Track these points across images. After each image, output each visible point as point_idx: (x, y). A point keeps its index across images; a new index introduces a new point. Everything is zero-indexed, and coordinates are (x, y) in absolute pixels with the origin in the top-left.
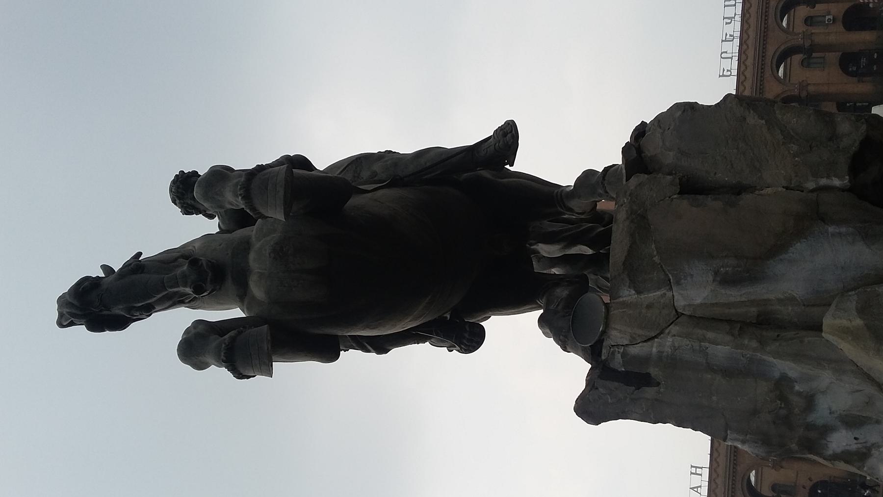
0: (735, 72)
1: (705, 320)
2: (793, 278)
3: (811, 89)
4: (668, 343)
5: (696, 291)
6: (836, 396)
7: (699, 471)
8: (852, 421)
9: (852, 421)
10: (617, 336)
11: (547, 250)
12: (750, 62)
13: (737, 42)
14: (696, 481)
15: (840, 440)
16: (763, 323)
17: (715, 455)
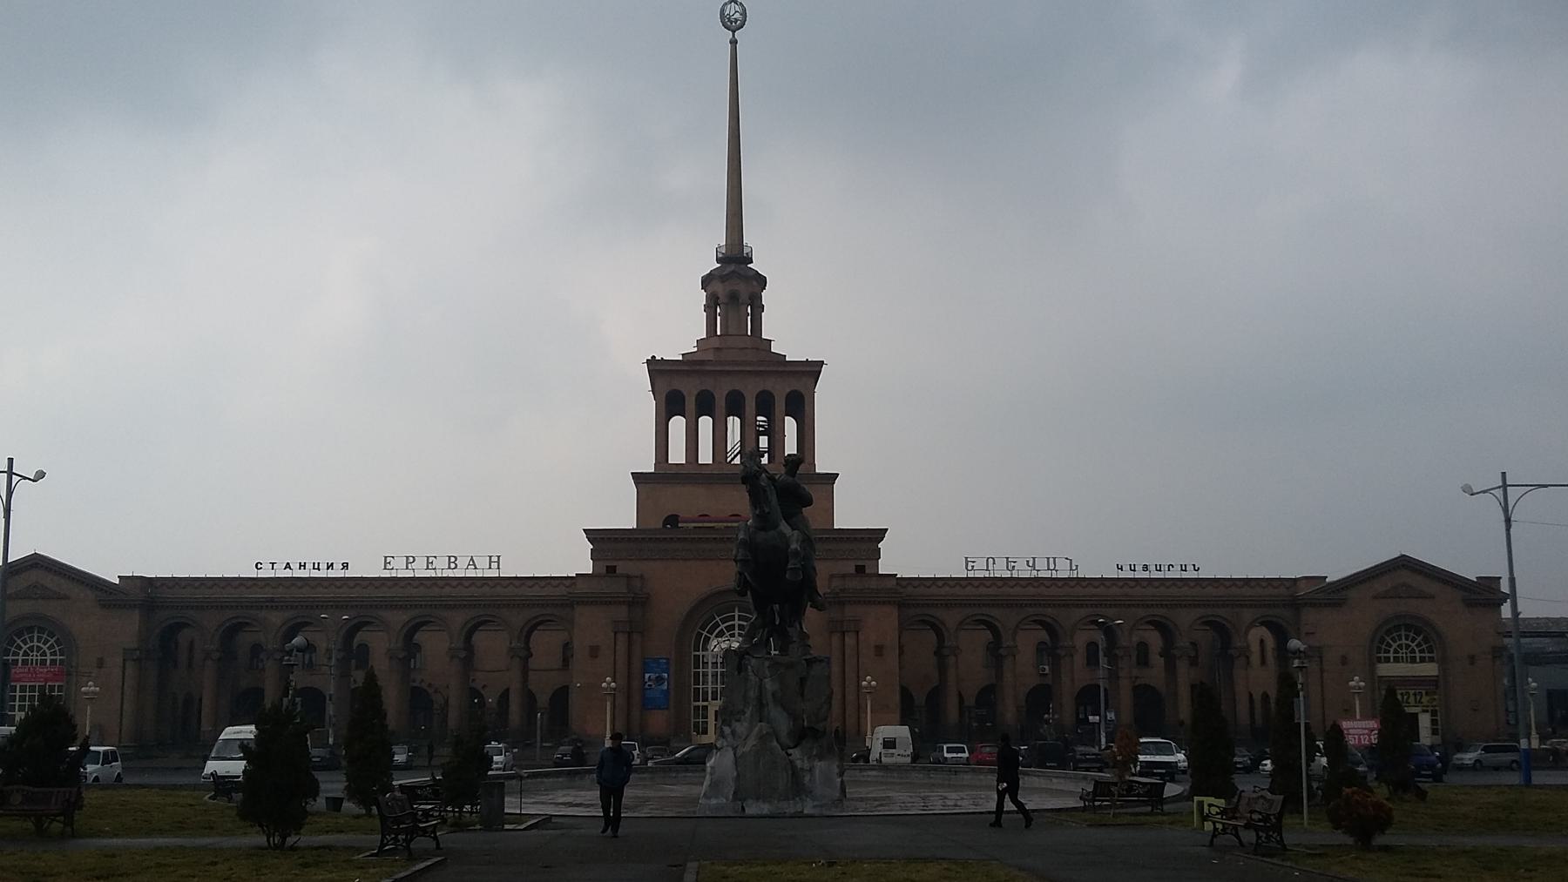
0: (971, 575)
1: (761, 688)
2: (776, 713)
3: (952, 660)
4: (752, 677)
5: (769, 685)
6: (741, 728)
7: (494, 565)
8: (733, 733)
9: (733, 733)
10: (753, 661)
11: (776, 607)
12: (983, 590)
14: (482, 563)
15: (727, 730)
16: (761, 705)
17: (517, 583)
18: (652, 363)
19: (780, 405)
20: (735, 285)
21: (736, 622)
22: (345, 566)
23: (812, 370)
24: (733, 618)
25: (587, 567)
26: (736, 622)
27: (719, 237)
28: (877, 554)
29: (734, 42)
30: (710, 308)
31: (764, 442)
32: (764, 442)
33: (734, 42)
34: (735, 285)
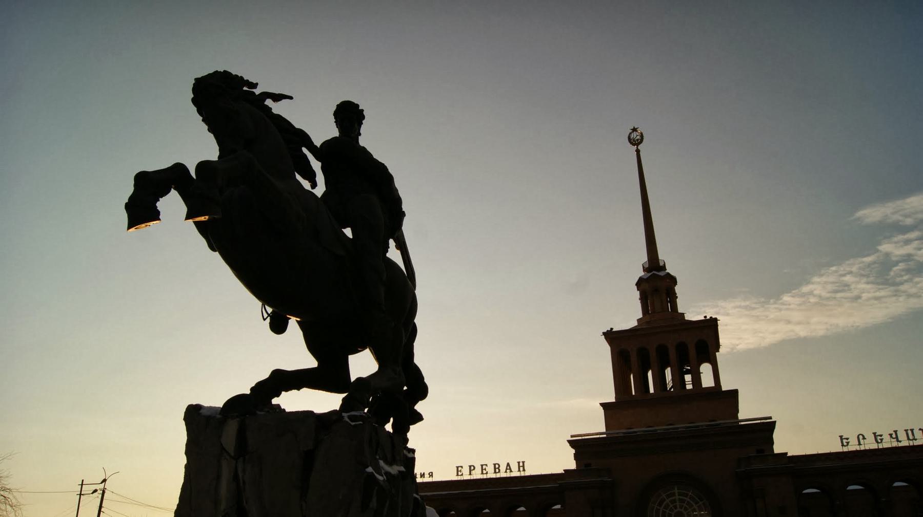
0: (845, 449)
13: (874, 446)
18: (604, 334)
19: (692, 353)
20: (657, 286)
21: (677, 497)
22: (431, 475)
23: (711, 325)
24: (674, 494)
25: (572, 465)
26: (677, 497)
27: (644, 258)
28: (771, 442)
29: (638, 151)
30: (644, 299)
31: (688, 378)
32: (688, 378)
33: (638, 151)
34: (657, 286)
